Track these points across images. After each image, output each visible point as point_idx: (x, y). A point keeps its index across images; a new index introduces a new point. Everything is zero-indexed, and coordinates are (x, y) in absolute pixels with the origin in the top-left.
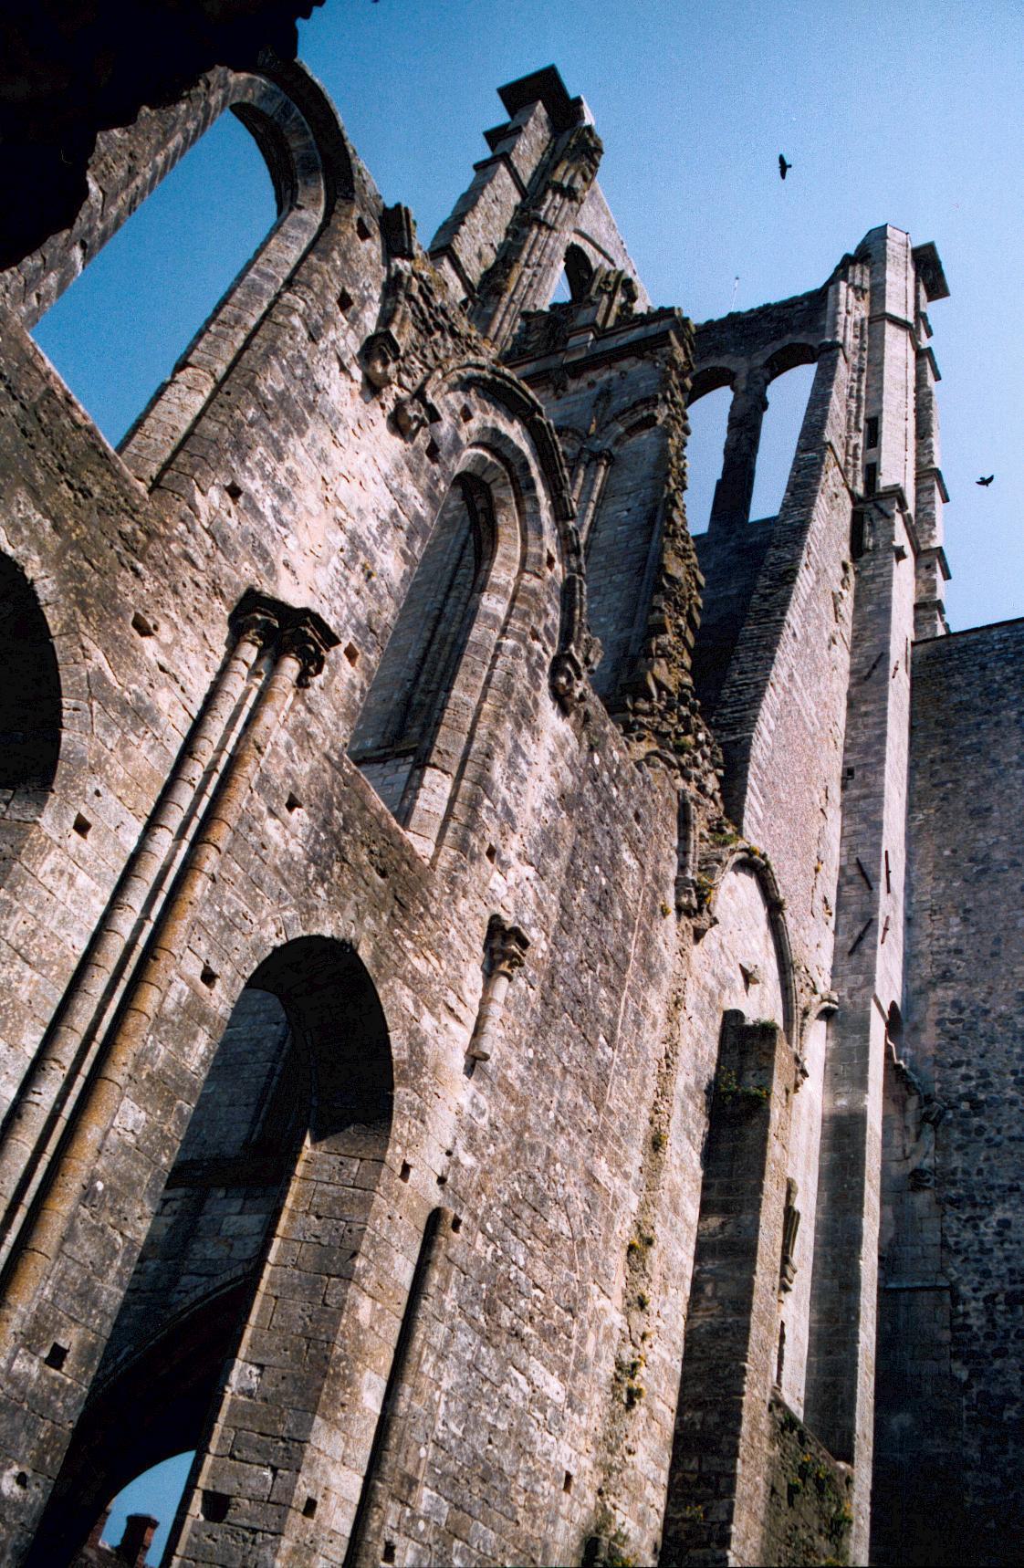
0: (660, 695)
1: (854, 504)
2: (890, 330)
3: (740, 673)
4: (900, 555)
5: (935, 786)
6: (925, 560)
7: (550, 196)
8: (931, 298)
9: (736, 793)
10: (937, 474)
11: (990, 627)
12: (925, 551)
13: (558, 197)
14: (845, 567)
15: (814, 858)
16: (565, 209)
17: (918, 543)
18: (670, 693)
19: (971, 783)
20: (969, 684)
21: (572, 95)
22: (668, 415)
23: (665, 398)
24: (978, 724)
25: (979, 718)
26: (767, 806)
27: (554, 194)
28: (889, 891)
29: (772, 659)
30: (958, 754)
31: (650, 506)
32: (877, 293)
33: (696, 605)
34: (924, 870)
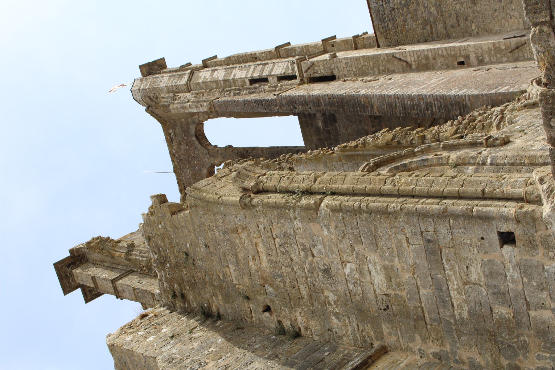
0: (460, 133)
1: (304, 83)
2: (194, 80)
3: (428, 110)
4: (334, 56)
5: (459, 25)
6: (329, 48)
7: (134, 257)
8: (166, 67)
9: (500, 98)
10: (277, 48)
11: (370, 8)
12: (324, 48)
13: (133, 253)
14: (345, 81)
15: (515, 69)
16: (140, 248)
17: (320, 52)
18: (458, 129)
19: (458, 6)
20: (402, 15)
21: (68, 254)
22: (286, 162)
23: (279, 164)
24: (425, 7)
25: (422, 8)
26: (502, 85)
27: (131, 255)
28: (524, 36)
29: (419, 95)
30: (442, 16)
31: (344, 161)
32: (175, 91)
33: (400, 130)
34: (506, 24)
